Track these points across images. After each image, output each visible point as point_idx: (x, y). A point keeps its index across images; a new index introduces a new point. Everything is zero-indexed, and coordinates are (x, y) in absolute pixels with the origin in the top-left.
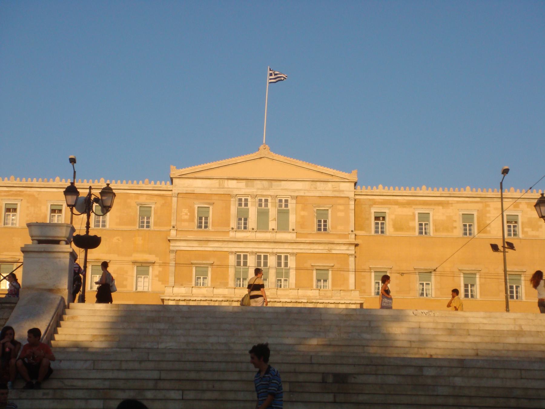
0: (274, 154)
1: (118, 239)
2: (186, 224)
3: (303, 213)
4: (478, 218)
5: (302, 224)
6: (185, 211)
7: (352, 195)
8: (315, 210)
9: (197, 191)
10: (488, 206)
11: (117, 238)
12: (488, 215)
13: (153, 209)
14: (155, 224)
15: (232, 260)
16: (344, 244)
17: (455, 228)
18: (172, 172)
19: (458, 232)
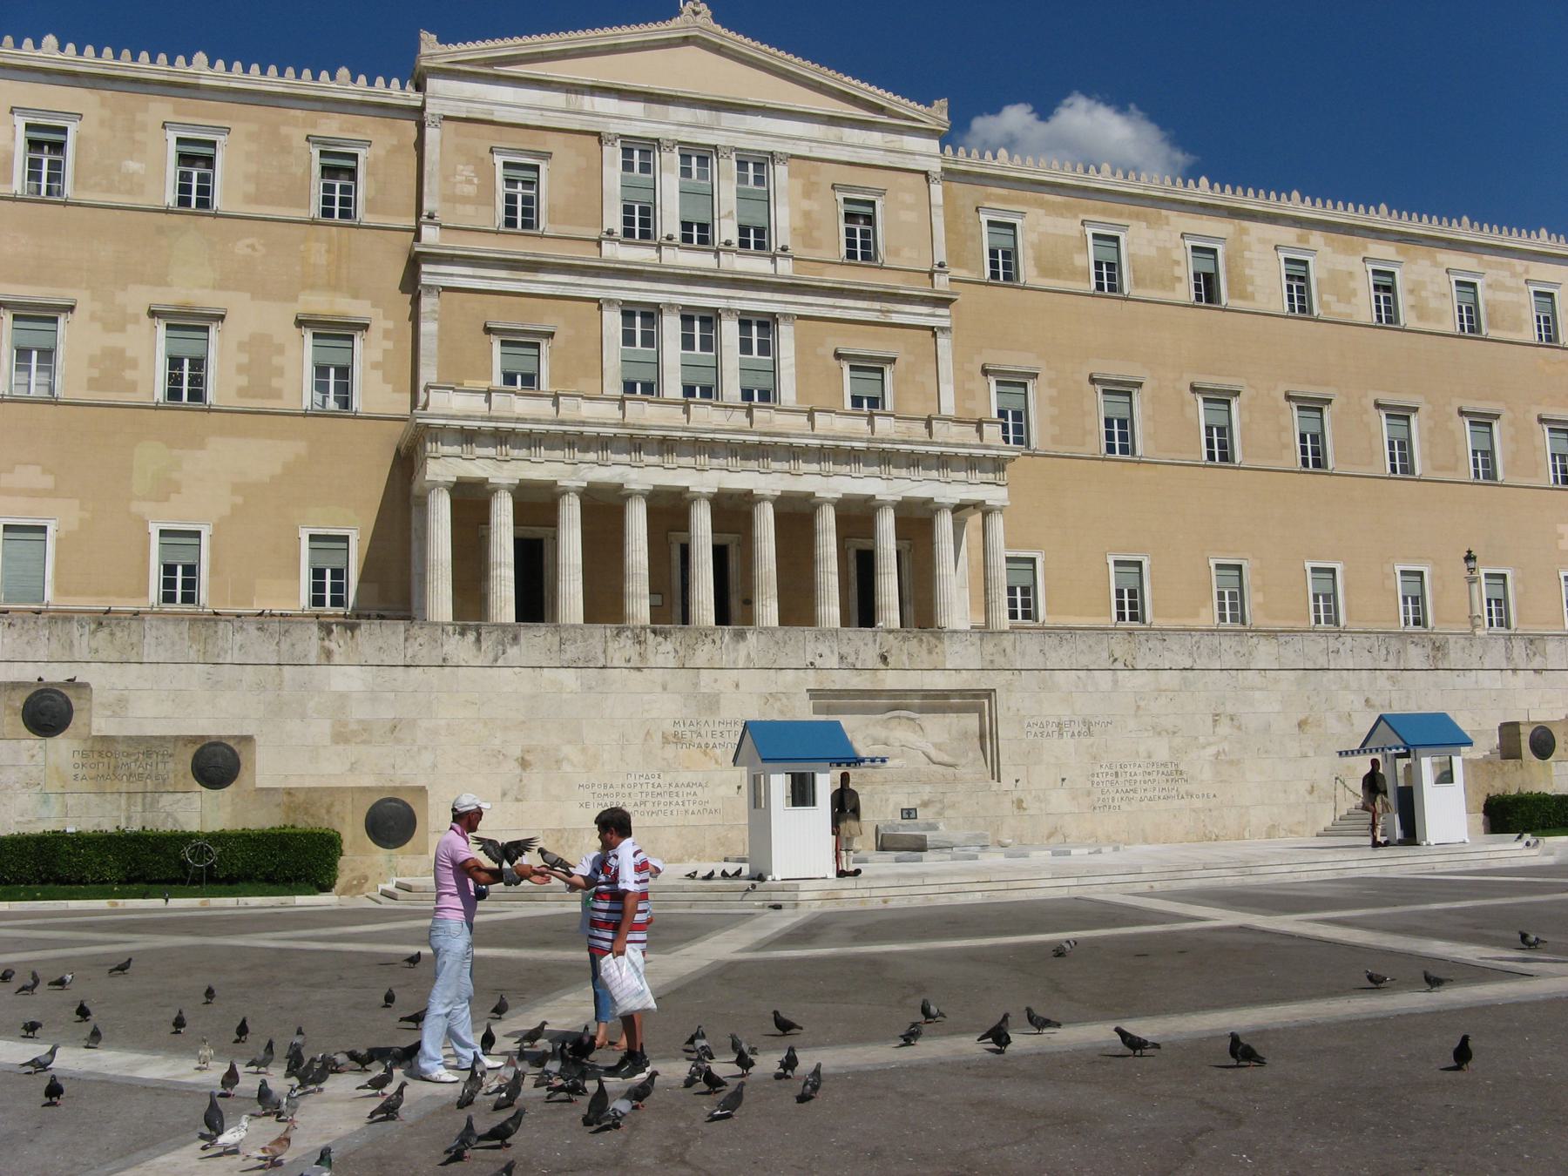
0: (724, 31)
1: (252, 247)
2: (469, 209)
3: (806, 205)
4: (1228, 259)
5: (806, 233)
6: (465, 171)
7: (935, 166)
8: (840, 196)
9: (501, 115)
10: (1244, 231)
11: (249, 241)
12: (1247, 254)
13: (360, 159)
14: (371, 207)
15: (613, 321)
16: (924, 301)
17: (1179, 279)
18: (424, 50)
19: (1185, 291)
